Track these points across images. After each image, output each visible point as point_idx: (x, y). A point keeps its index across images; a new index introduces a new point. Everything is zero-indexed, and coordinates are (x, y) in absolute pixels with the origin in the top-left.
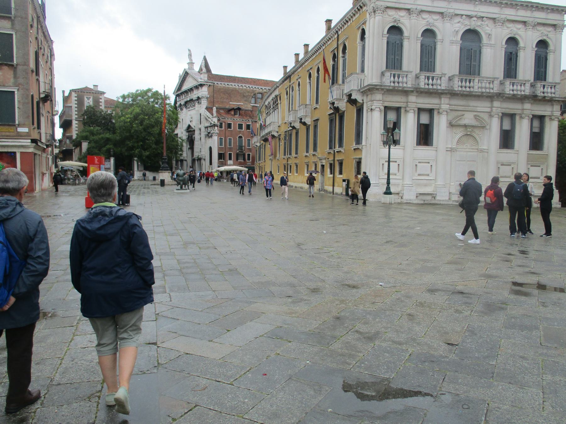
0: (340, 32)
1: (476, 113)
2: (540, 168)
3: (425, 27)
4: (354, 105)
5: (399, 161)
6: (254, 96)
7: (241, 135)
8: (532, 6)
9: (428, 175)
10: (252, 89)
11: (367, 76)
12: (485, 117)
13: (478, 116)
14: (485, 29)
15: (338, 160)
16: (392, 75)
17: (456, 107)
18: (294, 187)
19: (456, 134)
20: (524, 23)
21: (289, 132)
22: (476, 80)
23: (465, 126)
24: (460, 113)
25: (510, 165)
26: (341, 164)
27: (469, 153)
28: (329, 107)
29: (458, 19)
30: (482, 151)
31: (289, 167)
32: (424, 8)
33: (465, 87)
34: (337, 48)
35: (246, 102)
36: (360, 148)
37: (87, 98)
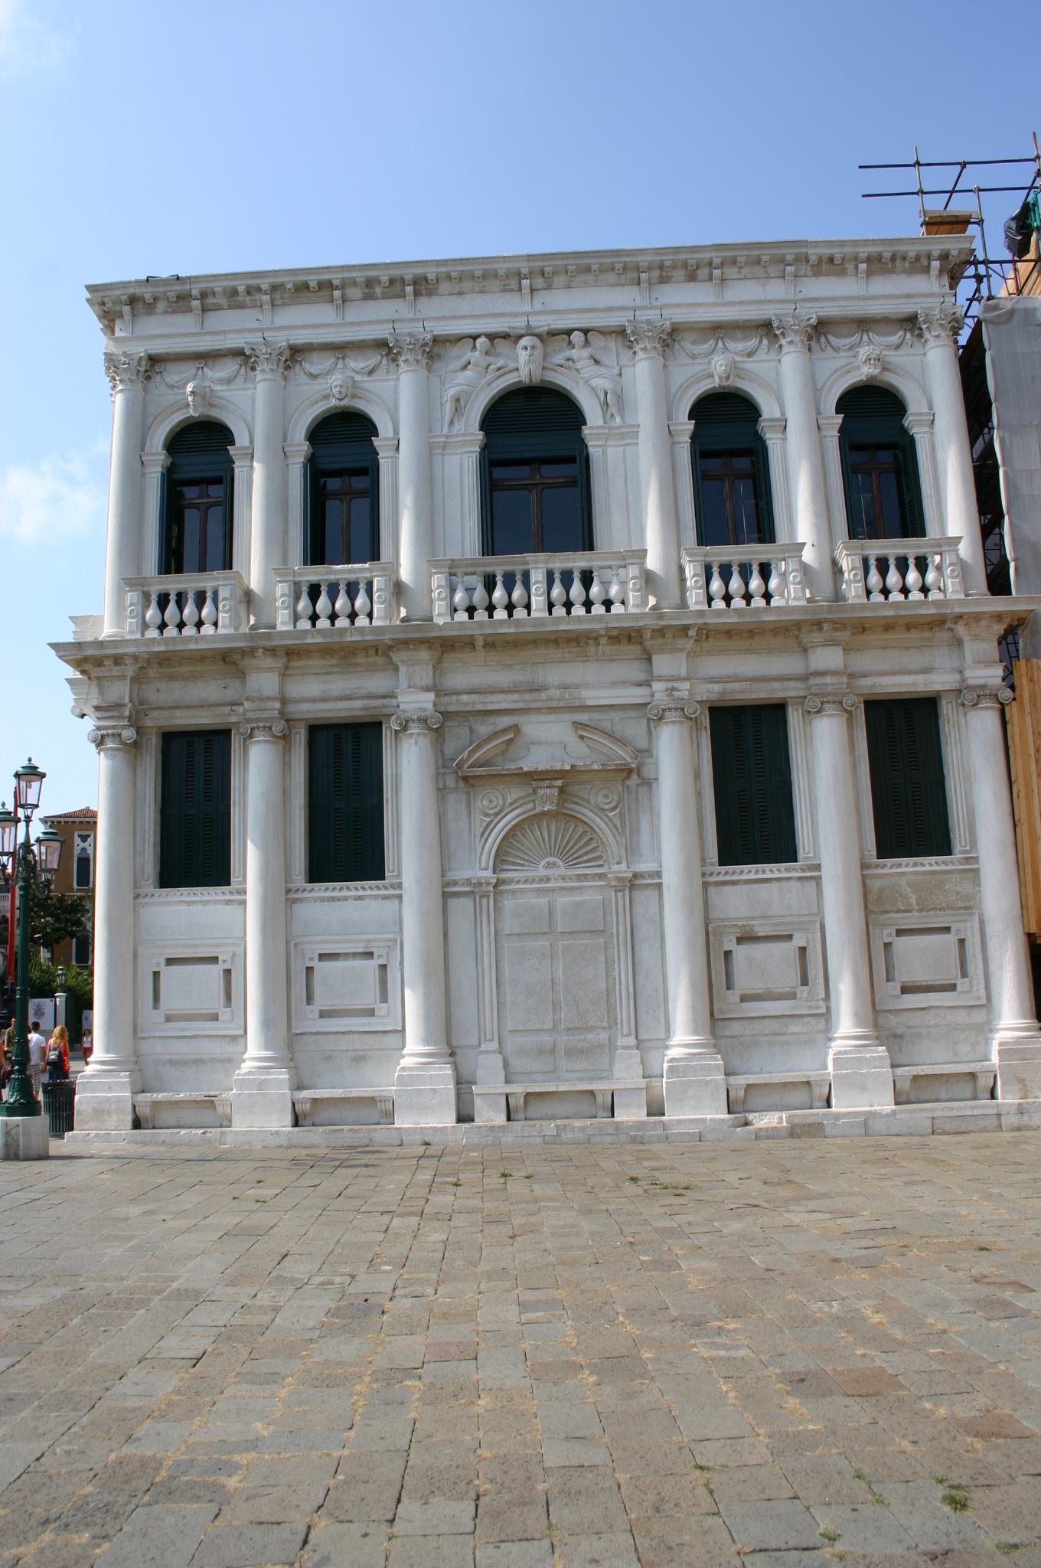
1: (583, 717)
2: (951, 939)
3: (321, 404)
5: (227, 957)
8: (781, 261)
9: (371, 1013)
12: (634, 729)
13: (584, 726)
17: (475, 697)
19: (487, 815)
20: (766, 328)
23: (534, 778)
24: (504, 721)
25: (790, 937)
27: (563, 901)
29: (464, 353)
30: (633, 883)
32: (301, 338)
37: (80, 836)
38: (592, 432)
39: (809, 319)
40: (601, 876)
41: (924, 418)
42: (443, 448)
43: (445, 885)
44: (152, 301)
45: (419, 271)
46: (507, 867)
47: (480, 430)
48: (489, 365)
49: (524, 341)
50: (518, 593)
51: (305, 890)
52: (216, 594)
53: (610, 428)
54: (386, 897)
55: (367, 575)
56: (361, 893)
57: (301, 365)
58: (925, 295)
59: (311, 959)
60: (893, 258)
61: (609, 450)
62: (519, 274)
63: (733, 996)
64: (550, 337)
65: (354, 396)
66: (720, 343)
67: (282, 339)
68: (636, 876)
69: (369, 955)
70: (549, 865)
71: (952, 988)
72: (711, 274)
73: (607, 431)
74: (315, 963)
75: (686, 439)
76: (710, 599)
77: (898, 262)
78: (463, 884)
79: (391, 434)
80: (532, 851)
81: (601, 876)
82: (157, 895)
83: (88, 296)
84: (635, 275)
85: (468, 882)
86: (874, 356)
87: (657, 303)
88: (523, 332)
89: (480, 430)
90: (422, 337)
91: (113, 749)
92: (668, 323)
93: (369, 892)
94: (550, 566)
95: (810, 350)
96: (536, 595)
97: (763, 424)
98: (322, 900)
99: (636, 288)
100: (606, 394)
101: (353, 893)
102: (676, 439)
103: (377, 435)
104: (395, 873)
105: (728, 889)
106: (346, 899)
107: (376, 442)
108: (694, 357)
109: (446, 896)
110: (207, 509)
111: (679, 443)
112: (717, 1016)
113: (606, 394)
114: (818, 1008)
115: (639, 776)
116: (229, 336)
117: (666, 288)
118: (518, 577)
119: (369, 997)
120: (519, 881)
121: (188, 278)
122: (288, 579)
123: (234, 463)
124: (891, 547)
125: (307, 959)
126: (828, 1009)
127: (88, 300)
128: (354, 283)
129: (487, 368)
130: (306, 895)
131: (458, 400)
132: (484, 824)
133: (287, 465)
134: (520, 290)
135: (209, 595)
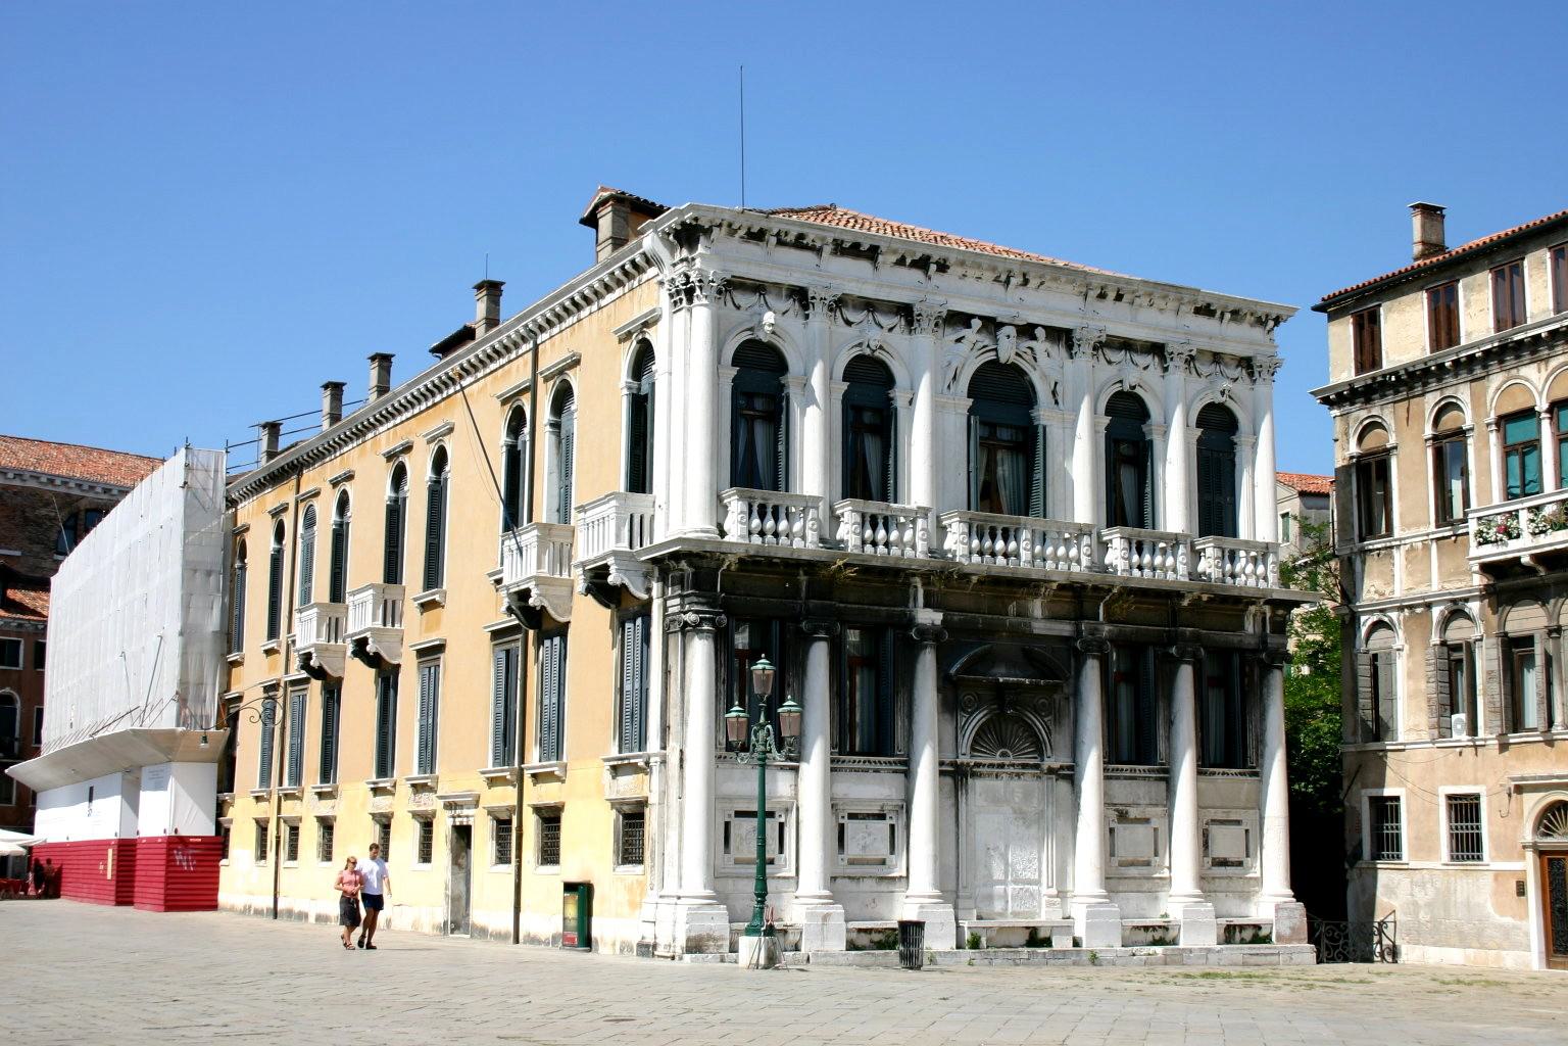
0: (545, 336)
2: (1239, 830)
4: (613, 606)
6: (71, 523)
7: (7, 690)
9: (883, 862)
10: (62, 490)
11: (664, 506)
14: (1045, 366)
15: (537, 810)
16: (755, 509)
18: (312, 919)
20: (1157, 350)
21: (290, 689)
22: (1025, 535)
26: (551, 818)
28: (506, 605)
31: (285, 831)
33: (993, 554)
34: (532, 389)
35: (36, 548)
36: (641, 763)
39: (1191, 351)
40: (1036, 766)
50: (1012, 545)
54: (895, 771)
56: (878, 766)
64: (1027, 331)
65: (881, 348)
68: (1062, 768)
69: (881, 817)
70: (1004, 755)
74: (845, 821)
81: (1036, 766)
88: (1007, 321)
93: (884, 767)
98: (851, 770)
101: (873, 766)
106: (867, 771)
108: (1109, 362)
109: (942, 773)
113: (1056, 384)
119: (882, 850)
132: (964, 719)
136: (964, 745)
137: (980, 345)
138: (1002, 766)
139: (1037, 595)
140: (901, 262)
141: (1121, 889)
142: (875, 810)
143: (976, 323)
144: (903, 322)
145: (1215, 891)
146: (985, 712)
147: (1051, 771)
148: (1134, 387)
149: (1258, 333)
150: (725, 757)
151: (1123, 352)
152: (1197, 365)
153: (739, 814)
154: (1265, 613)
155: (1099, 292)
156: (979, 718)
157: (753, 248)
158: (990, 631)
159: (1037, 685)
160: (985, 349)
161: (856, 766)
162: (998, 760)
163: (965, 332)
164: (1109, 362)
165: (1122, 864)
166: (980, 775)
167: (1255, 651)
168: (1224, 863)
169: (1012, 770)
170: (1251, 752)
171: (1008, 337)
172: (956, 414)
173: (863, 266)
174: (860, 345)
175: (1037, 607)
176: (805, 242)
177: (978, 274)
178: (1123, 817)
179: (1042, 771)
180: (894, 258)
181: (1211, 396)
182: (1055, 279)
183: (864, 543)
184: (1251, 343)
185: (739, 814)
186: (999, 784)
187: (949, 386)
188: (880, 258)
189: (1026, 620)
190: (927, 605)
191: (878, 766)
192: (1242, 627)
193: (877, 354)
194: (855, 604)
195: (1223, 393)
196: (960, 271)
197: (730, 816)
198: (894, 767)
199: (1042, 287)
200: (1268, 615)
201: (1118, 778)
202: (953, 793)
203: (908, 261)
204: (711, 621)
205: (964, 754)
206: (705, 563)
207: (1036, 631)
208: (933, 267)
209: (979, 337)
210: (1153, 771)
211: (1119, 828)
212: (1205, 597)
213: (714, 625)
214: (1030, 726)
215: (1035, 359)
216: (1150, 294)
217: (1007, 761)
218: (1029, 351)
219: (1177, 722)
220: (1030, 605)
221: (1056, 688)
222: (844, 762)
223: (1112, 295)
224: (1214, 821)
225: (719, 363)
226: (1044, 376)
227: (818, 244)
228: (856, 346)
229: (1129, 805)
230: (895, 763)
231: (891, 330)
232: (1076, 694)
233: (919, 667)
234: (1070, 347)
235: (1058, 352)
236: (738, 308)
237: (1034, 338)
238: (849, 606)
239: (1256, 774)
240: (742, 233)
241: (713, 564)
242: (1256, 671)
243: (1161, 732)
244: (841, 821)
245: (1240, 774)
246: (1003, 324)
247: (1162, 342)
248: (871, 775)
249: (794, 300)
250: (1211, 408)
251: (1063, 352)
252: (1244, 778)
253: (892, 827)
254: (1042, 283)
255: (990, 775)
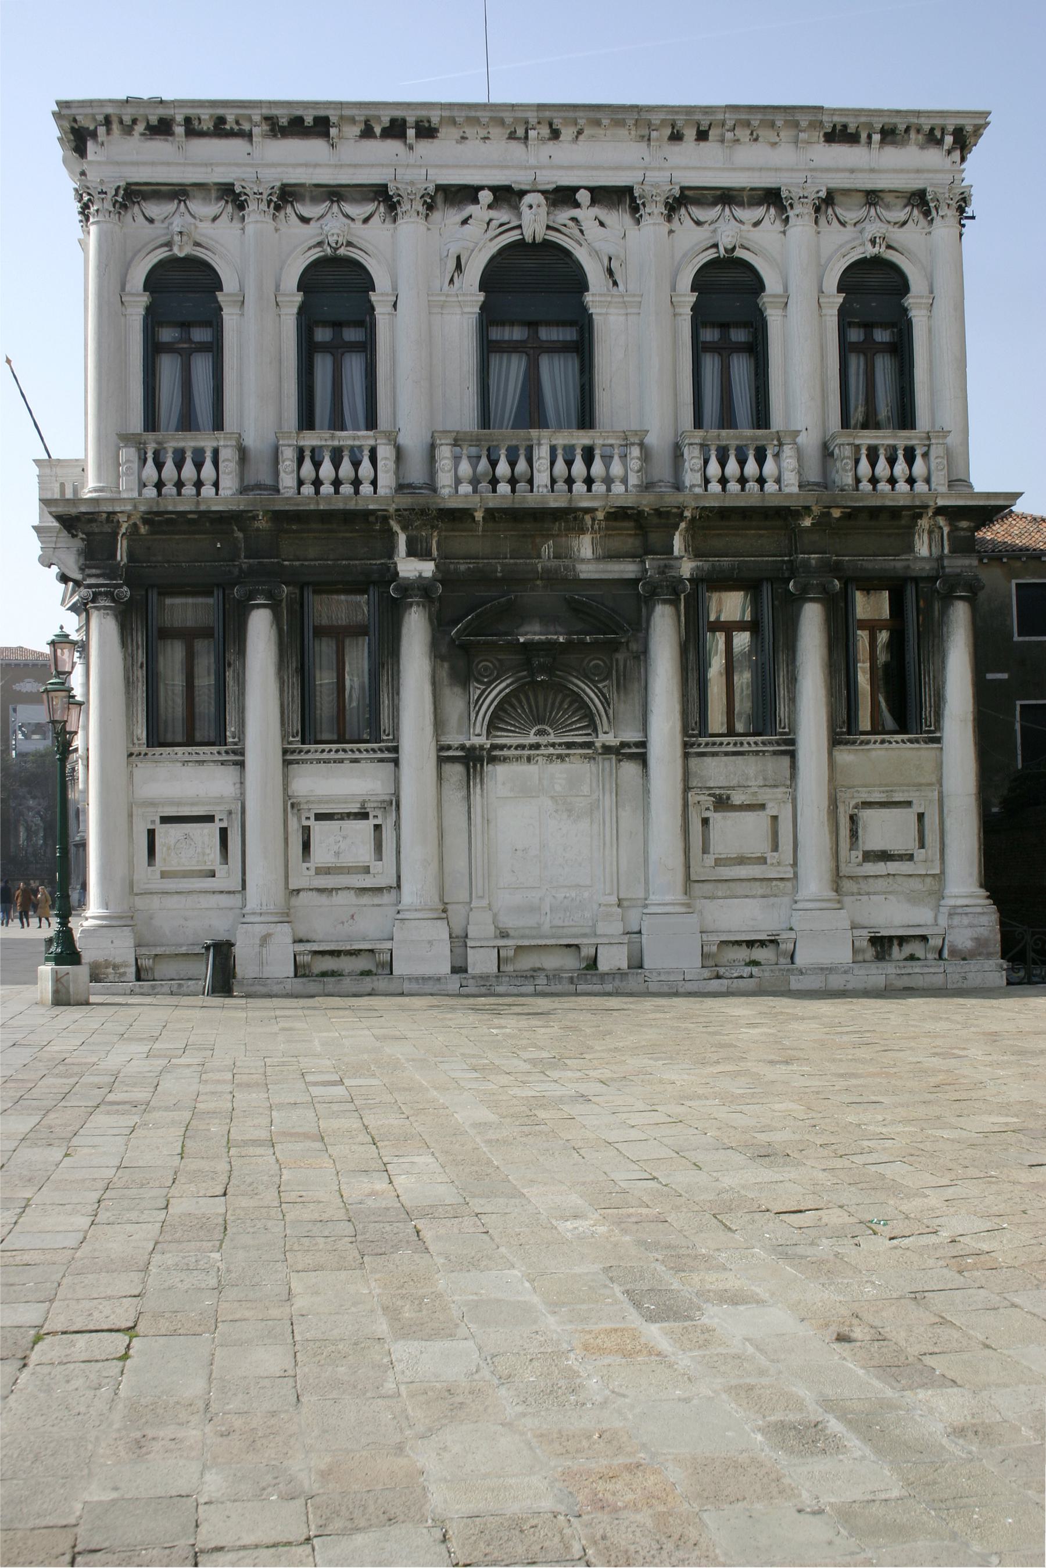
38: (597, 299)
39: (818, 192)
41: (924, 301)
42: (442, 307)
43: (441, 748)
44: (129, 123)
45: (423, 113)
46: (499, 734)
47: (480, 291)
48: (491, 220)
49: (528, 199)
51: (301, 751)
52: (216, 452)
53: (612, 296)
54: (381, 760)
55: (372, 442)
56: (357, 755)
57: (293, 206)
58: (936, 171)
59: (308, 818)
60: (907, 130)
61: (612, 318)
62: (527, 123)
63: (710, 860)
65: (350, 244)
66: (727, 209)
67: (275, 177)
68: (624, 745)
69: (364, 816)
70: (540, 733)
71: (910, 857)
72: (723, 136)
73: (609, 299)
74: (312, 823)
75: (687, 312)
76: (707, 481)
77: (913, 135)
78: (457, 749)
79: (388, 289)
80: (523, 719)
82: (150, 754)
83: (56, 108)
84: (646, 132)
85: (462, 747)
86: (879, 235)
87: (667, 165)
88: (527, 188)
89: (480, 291)
90: (425, 186)
91: (106, 608)
92: (678, 188)
93: (365, 755)
94: (554, 442)
95: (816, 223)
96: (539, 471)
97: (765, 300)
98: (319, 761)
99: (644, 145)
100: (610, 259)
101: (349, 755)
102: (678, 310)
103: (374, 290)
104: (391, 737)
105: (708, 760)
106: (341, 761)
107: (373, 297)
108: (698, 223)
109: (441, 761)
110: (190, 355)
111: (681, 315)
112: (693, 877)
113: (610, 259)
114: (785, 872)
115: (628, 649)
116: (217, 169)
117: (676, 148)
118: (522, 452)
119: (364, 853)
120: (510, 747)
121: (173, 102)
122: (290, 442)
123: (221, 310)
124: (883, 438)
125: (303, 818)
126: (796, 874)
127: (54, 114)
128: (352, 120)
129: (488, 224)
130: (303, 756)
131: (458, 258)
132: (478, 692)
133: (279, 315)
134: (526, 138)
135: (209, 455)
136: (478, 724)
137: (495, 223)
138: (537, 746)
139: (582, 530)
140: (367, 133)
141: (720, 894)
142: (355, 808)
143: (486, 197)
144: (382, 209)
145: (868, 894)
146: (508, 681)
147: (607, 749)
148: (734, 249)
149: (934, 157)
150: (146, 754)
151: (719, 207)
152: (838, 210)
153: (165, 820)
154: (941, 528)
155: (668, 132)
156: (500, 688)
157: (160, 147)
158: (514, 580)
159: (582, 643)
160: (504, 228)
161: (325, 756)
162: (532, 739)
163: (471, 209)
164: (698, 223)
165: (719, 862)
166: (505, 759)
167: (933, 579)
168: (884, 856)
169: (551, 750)
170: (928, 712)
171: (531, 207)
172: (463, 313)
173: (313, 148)
174: (320, 244)
175: (585, 546)
176: (228, 127)
177: (483, 133)
178: (722, 803)
179: (596, 749)
180: (357, 130)
181: (861, 249)
182: (597, 123)
183: (300, 483)
184: (918, 171)
185: (165, 820)
186: (532, 769)
187: (452, 281)
188: (333, 131)
189: (567, 562)
190: (411, 553)
191: (357, 755)
192: (910, 548)
193: (342, 251)
194: (316, 560)
195: (873, 242)
196: (455, 133)
197: (153, 822)
198: (379, 755)
199: (581, 137)
200: (946, 530)
201: (714, 754)
202: (465, 784)
203: (378, 130)
204: (109, 595)
205: (479, 735)
206: (95, 528)
207: (582, 576)
208: (411, 133)
209: (492, 214)
210: (770, 743)
211: (717, 819)
212: (836, 513)
213: (114, 600)
214: (579, 695)
215: (582, 231)
216: (747, 124)
217: (543, 740)
218: (571, 224)
219: (800, 678)
220: (575, 543)
221: (614, 647)
222: (308, 752)
223: (690, 133)
224: (867, 805)
225: (123, 289)
226: (595, 253)
227: (246, 127)
228: (314, 246)
229: (733, 788)
230: (381, 750)
231: (366, 220)
232: (642, 656)
233: (405, 631)
234: (635, 209)
235: (617, 219)
236: (151, 221)
237: (577, 205)
238: (306, 563)
239: (938, 740)
240: (140, 128)
241: (107, 529)
242: (937, 606)
243: (782, 692)
244: (305, 823)
245: (911, 741)
246: (522, 193)
247: (773, 186)
248: (347, 765)
249: (227, 202)
250: (876, 264)
251: (627, 218)
252: (916, 745)
253: (377, 828)
254: (580, 132)
255: (518, 758)
